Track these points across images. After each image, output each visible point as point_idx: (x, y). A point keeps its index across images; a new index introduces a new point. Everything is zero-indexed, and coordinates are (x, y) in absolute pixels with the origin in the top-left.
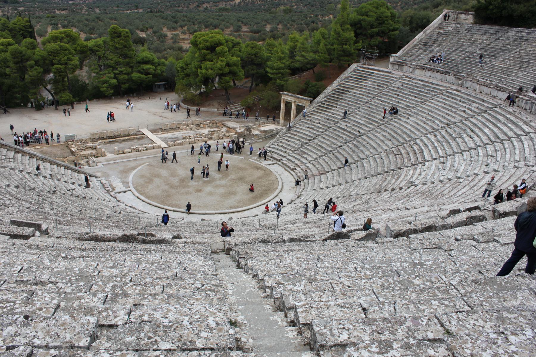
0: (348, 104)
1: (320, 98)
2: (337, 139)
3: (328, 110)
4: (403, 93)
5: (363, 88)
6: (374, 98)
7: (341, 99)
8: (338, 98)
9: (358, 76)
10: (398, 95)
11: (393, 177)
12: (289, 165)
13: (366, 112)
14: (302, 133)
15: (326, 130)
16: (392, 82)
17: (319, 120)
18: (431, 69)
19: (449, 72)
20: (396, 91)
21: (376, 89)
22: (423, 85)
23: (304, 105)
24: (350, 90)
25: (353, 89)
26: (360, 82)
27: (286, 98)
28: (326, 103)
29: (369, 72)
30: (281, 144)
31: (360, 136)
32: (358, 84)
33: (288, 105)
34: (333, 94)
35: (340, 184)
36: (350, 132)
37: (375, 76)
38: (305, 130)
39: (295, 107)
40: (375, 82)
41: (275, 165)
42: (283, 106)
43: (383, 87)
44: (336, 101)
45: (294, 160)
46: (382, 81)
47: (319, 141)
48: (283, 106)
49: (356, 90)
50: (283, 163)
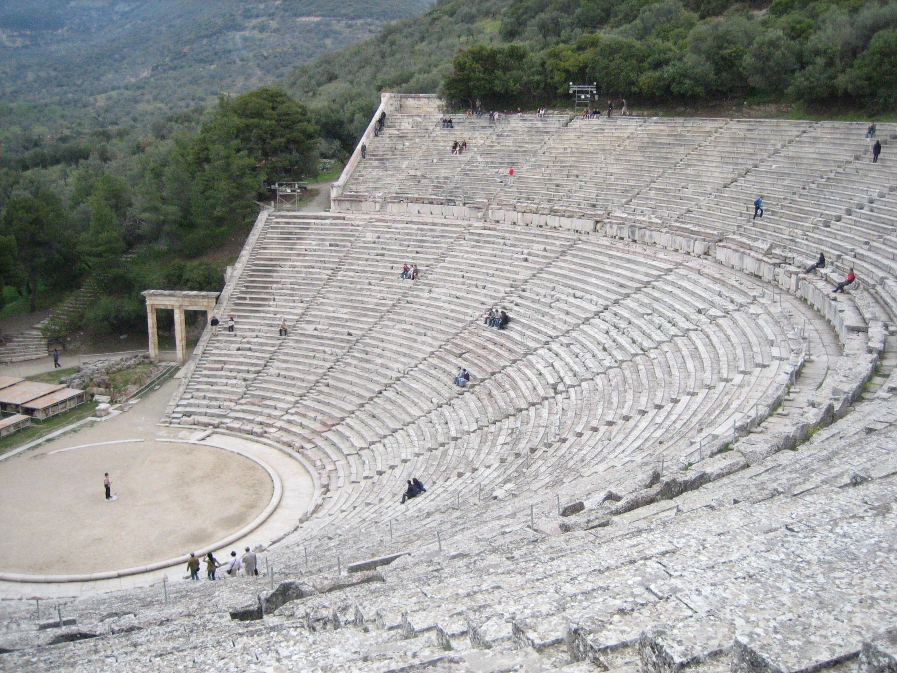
2: (314, 357)
9: (281, 233)
14: (231, 363)
18: (417, 199)
19: (453, 201)
22: (418, 229)
23: (203, 309)
24: (281, 263)
27: (156, 302)
28: (248, 296)
29: (300, 223)
34: (251, 276)
36: (332, 339)
37: (316, 229)
38: (236, 356)
39: (183, 317)
40: (324, 240)
43: (344, 246)
45: (250, 417)
47: (278, 368)
48: (152, 321)
50: (228, 428)
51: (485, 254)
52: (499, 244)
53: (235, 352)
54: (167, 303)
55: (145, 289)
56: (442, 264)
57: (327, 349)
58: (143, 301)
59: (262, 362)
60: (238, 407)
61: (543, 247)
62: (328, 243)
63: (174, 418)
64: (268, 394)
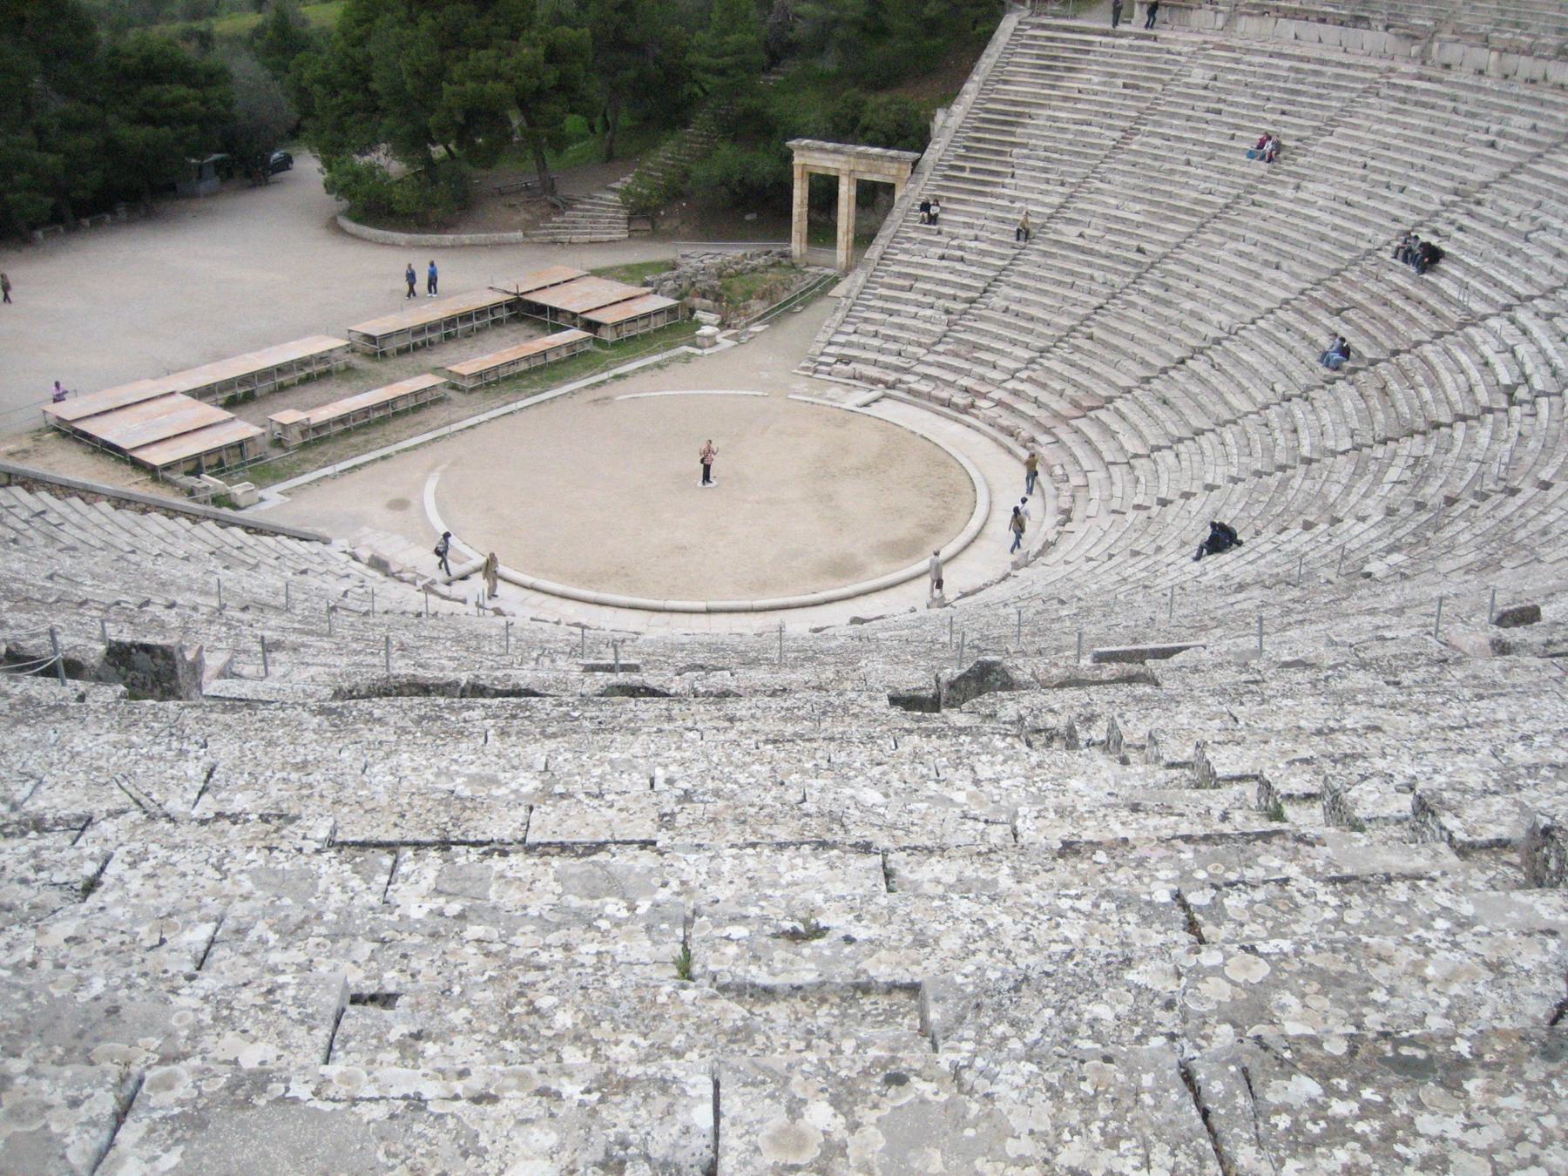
2: (1073, 284)
3: (988, 189)
7: (1013, 144)
8: (1003, 143)
9: (1039, 57)
19: (1365, 19)
22: (1291, 69)
23: (889, 180)
24: (1033, 111)
27: (809, 162)
28: (968, 165)
34: (977, 129)
36: (1108, 257)
37: (1103, 54)
38: (936, 268)
39: (853, 193)
40: (1114, 75)
42: (800, 193)
43: (1150, 90)
45: (950, 377)
47: (1006, 298)
48: (800, 193)
50: (910, 391)
51: (1413, 127)
52: (1443, 109)
53: (935, 262)
54: (829, 164)
56: (1328, 139)
57: (1097, 274)
58: (788, 157)
59: (981, 285)
60: (931, 358)
61: (1528, 122)
62: (1120, 82)
63: (821, 363)
64: (984, 341)
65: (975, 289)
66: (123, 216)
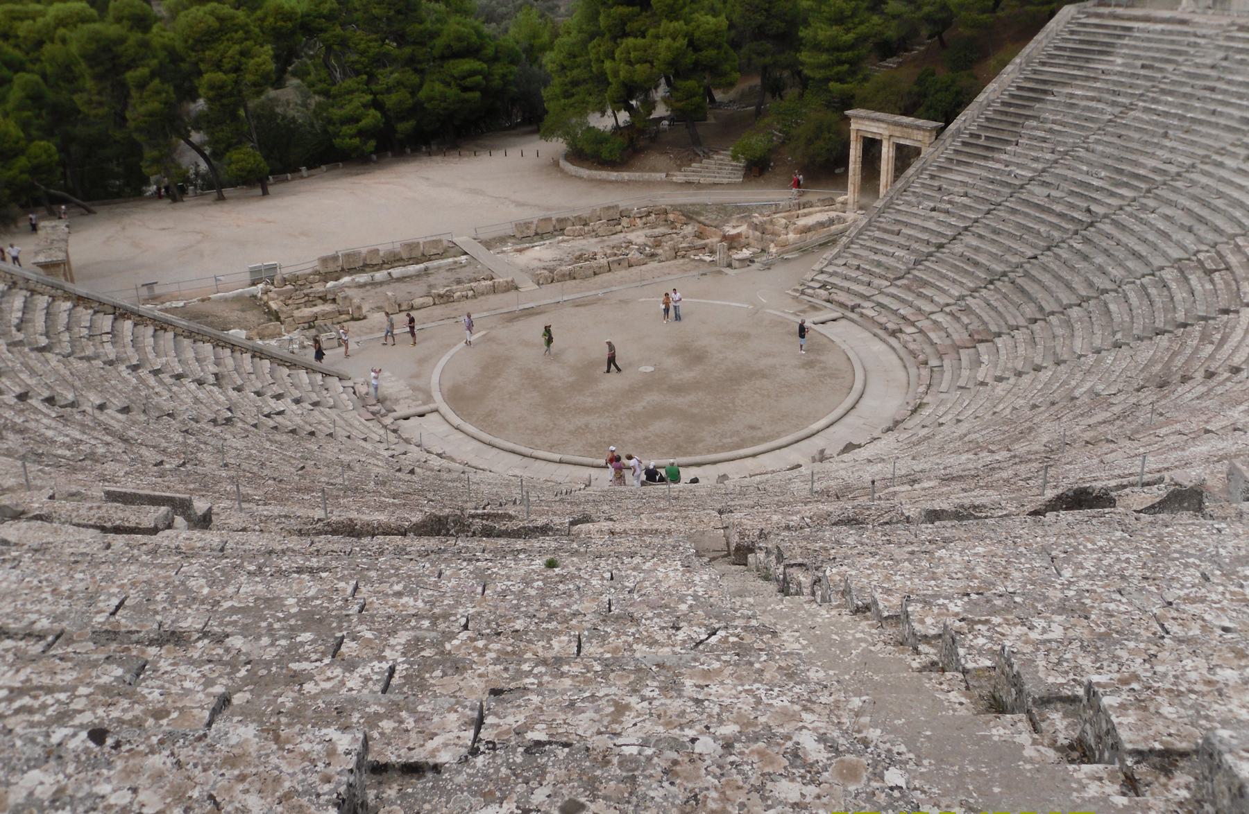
0: (1051, 131)
1: (967, 119)
4: (1230, 82)
5: (1095, 79)
6: (1131, 107)
10: (1213, 89)
11: (1205, 338)
12: (882, 320)
13: (1108, 150)
15: (988, 212)
16: (1192, 51)
17: (965, 184)
20: (1206, 77)
21: (1138, 76)
23: (917, 144)
24: (1055, 89)
25: (1065, 84)
26: (1087, 60)
27: (863, 128)
29: (1115, 27)
30: (856, 262)
31: (1092, 224)
32: (1080, 68)
33: (871, 147)
35: (1038, 369)
36: (1061, 215)
37: (1136, 38)
38: (926, 219)
39: (892, 153)
40: (1137, 57)
41: (844, 322)
42: (855, 152)
43: (1161, 70)
44: (1014, 124)
45: (894, 305)
46: (1158, 50)
47: (967, 246)
48: (855, 152)
49: (1078, 87)
50: (862, 315)
55: (850, 109)
59: (949, 233)
60: (893, 290)
62: (1139, 63)
63: (809, 287)
65: (944, 235)
66: (434, 148)
